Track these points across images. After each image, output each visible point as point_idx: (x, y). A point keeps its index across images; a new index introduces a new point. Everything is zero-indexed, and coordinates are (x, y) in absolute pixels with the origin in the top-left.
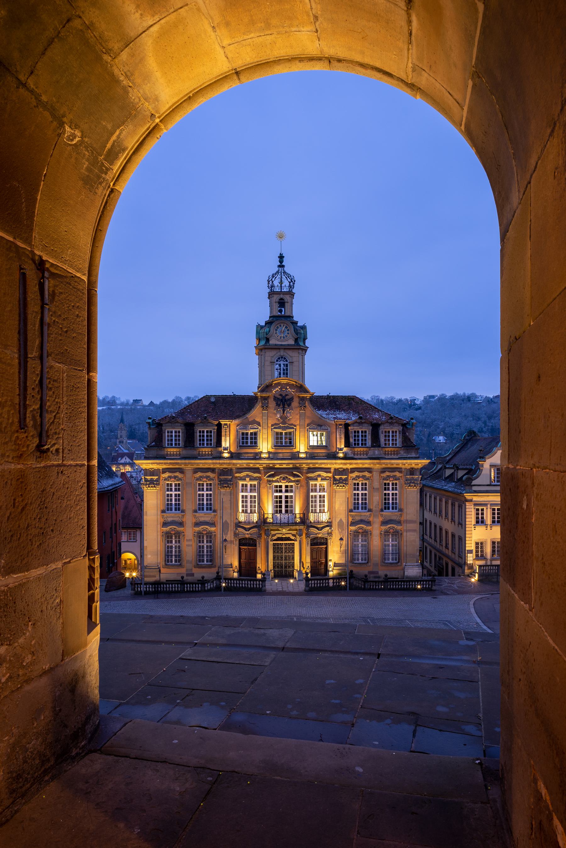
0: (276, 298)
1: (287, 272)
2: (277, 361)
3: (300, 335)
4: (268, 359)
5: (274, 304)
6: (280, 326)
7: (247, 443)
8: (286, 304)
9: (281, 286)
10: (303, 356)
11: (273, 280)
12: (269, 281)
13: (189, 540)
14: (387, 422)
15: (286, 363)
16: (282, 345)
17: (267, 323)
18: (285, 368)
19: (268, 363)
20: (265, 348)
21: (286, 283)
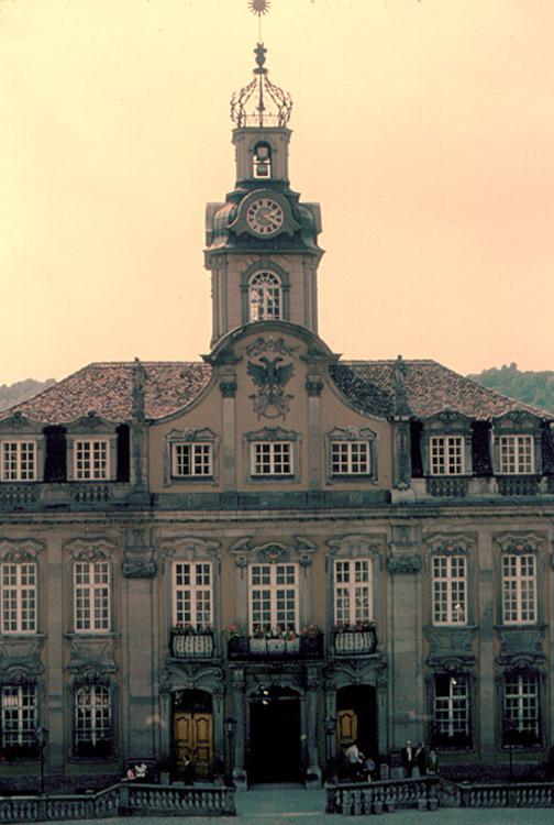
0: (250, 140)
1: (273, 83)
2: (254, 282)
9: (261, 116)
11: (243, 101)
12: (233, 105)
13: (56, 698)
15: (275, 286)
17: (230, 198)
18: (271, 298)
21: (272, 107)
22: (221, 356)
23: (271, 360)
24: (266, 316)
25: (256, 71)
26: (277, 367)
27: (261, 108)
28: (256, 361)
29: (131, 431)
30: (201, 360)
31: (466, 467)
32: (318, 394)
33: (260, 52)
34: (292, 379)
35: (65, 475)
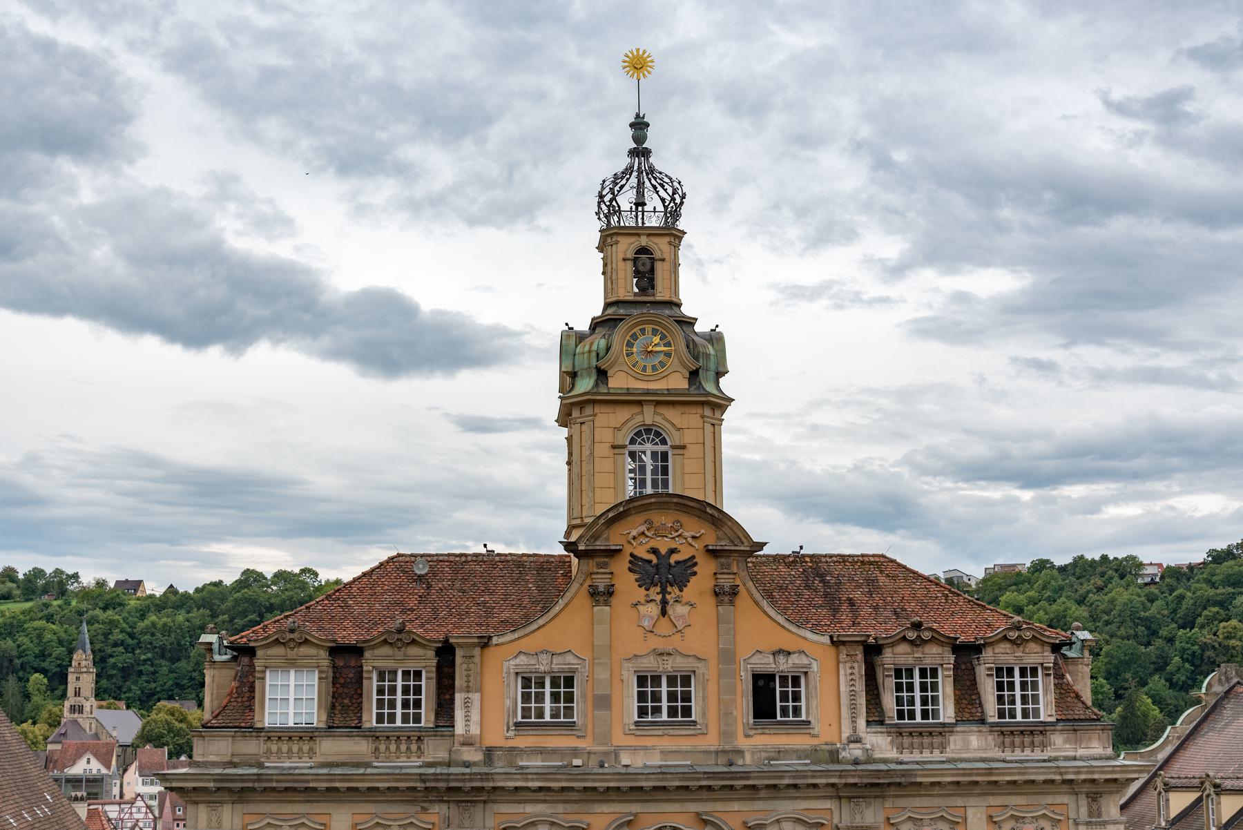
0: (626, 247)
2: (633, 441)
3: (703, 359)
4: (605, 437)
5: (621, 264)
6: (643, 331)
7: (540, 714)
8: (658, 265)
10: (716, 425)
12: (601, 196)
14: (1005, 638)
16: (648, 392)
17: (596, 324)
19: (603, 449)
20: (594, 402)
22: (590, 545)
23: (663, 551)
24: (649, 490)
25: (633, 153)
26: (672, 561)
27: (640, 203)
28: (642, 552)
29: (459, 653)
30: (560, 551)
31: (947, 711)
32: (732, 603)
33: (640, 126)
34: (693, 579)
35: (360, 718)
